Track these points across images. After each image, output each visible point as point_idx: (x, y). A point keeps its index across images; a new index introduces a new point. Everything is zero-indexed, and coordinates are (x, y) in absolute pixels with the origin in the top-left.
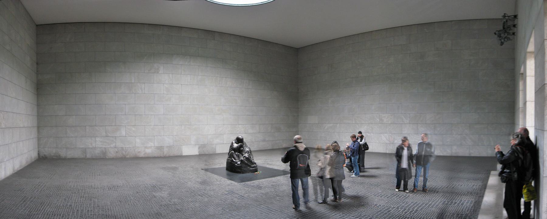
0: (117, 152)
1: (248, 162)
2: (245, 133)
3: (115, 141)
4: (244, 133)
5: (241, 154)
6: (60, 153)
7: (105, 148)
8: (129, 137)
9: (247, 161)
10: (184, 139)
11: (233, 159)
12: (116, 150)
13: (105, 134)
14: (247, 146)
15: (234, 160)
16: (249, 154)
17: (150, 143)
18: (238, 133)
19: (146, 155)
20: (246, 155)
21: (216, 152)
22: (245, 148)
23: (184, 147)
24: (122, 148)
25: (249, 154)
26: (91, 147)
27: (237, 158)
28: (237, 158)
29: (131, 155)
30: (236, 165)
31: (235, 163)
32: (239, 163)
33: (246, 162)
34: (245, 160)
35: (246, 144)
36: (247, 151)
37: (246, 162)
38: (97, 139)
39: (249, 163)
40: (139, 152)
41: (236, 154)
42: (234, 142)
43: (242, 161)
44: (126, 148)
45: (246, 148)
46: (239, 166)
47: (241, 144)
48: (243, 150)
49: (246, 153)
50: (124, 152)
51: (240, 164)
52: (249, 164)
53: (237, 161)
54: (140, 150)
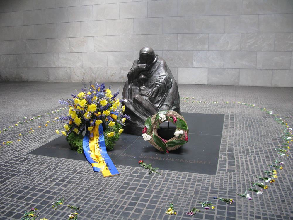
0: (84, 74)
3: (81, 58)
6: (22, 74)
7: (69, 68)
8: (99, 53)
9: (134, 107)
10: (181, 57)
12: (83, 70)
13: (69, 49)
17: (128, 62)
19: (122, 79)
21: (239, 83)
23: (181, 69)
24: (90, 68)
26: (54, 66)
29: (103, 78)
38: (59, 56)
40: (113, 75)
44: (96, 68)
50: (93, 74)
54: (114, 72)
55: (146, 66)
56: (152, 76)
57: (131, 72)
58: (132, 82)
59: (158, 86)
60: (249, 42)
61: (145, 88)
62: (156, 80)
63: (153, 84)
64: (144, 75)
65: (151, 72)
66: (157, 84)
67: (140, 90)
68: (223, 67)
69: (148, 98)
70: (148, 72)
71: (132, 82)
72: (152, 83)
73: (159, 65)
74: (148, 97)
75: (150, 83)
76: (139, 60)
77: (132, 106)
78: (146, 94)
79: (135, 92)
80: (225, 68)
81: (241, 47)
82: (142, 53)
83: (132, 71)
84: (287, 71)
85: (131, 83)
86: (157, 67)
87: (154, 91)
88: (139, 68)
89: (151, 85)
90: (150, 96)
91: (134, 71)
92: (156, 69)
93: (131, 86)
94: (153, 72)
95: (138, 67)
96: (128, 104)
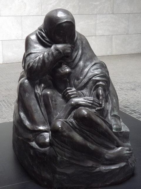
1: (85, 138)
2: (113, 13)
4: (111, 13)
5: (60, 91)
9: (81, 134)
11: (22, 115)
14: (93, 56)
15: (27, 123)
16: (98, 96)
18: (95, 13)
20: (81, 100)
22: (81, 63)
25: (98, 96)
27: (38, 112)
28: (38, 112)
30: (34, 144)
31: (30, 136)
32: (47, 137)
33: (78, 138)
34: (74, 128)
35: (87, 46)
36: (90, 79)
37: (78, 138)
39: (93, 142)
41: (36, 94)
42: (34, 37)
43: (55, 132)
45: (85, 67)
46: (44, 153)
47: (60, 46)
48: (69, 74)
49: (85, 86)
51: (51, 144)
52: (93, 147)
53: (41, 128)
55: (71, 47)
56: (77, 65)
57: (41, 62)
58: (38, 81)
59: (100, 84)
60: (51, 4)
61: (76, 91)
62: (90, 74)
63: (87, 83)
64: (69, 65)
65: (74, 57)
66: (98, 81)
67: (67, 98)
68: (20, 38)
69: (94, 110)
70: (70, 61)
71: (38, 81)
72: (86, 80)
73: (82, 42)
74: (95, 108)
75: (78, 79)
76: (44, 35)
77: (76, 133)
78: (89, 103)
79: (55, 101)
80: (23, 39)
81: (42, 10)
82: (60, 22)
83: (43, 60)
84: (94, 37)
85: (40, 85)
86: (80, 48)
87: (102, 95)
88: (60, 52)
89: (82, 84)
90: (98, 107)
91: (48, 58)
92: (80, 52)
93: (43, 90)
94: (78, 57)
95: (57, 50)
96: (71, 131)
